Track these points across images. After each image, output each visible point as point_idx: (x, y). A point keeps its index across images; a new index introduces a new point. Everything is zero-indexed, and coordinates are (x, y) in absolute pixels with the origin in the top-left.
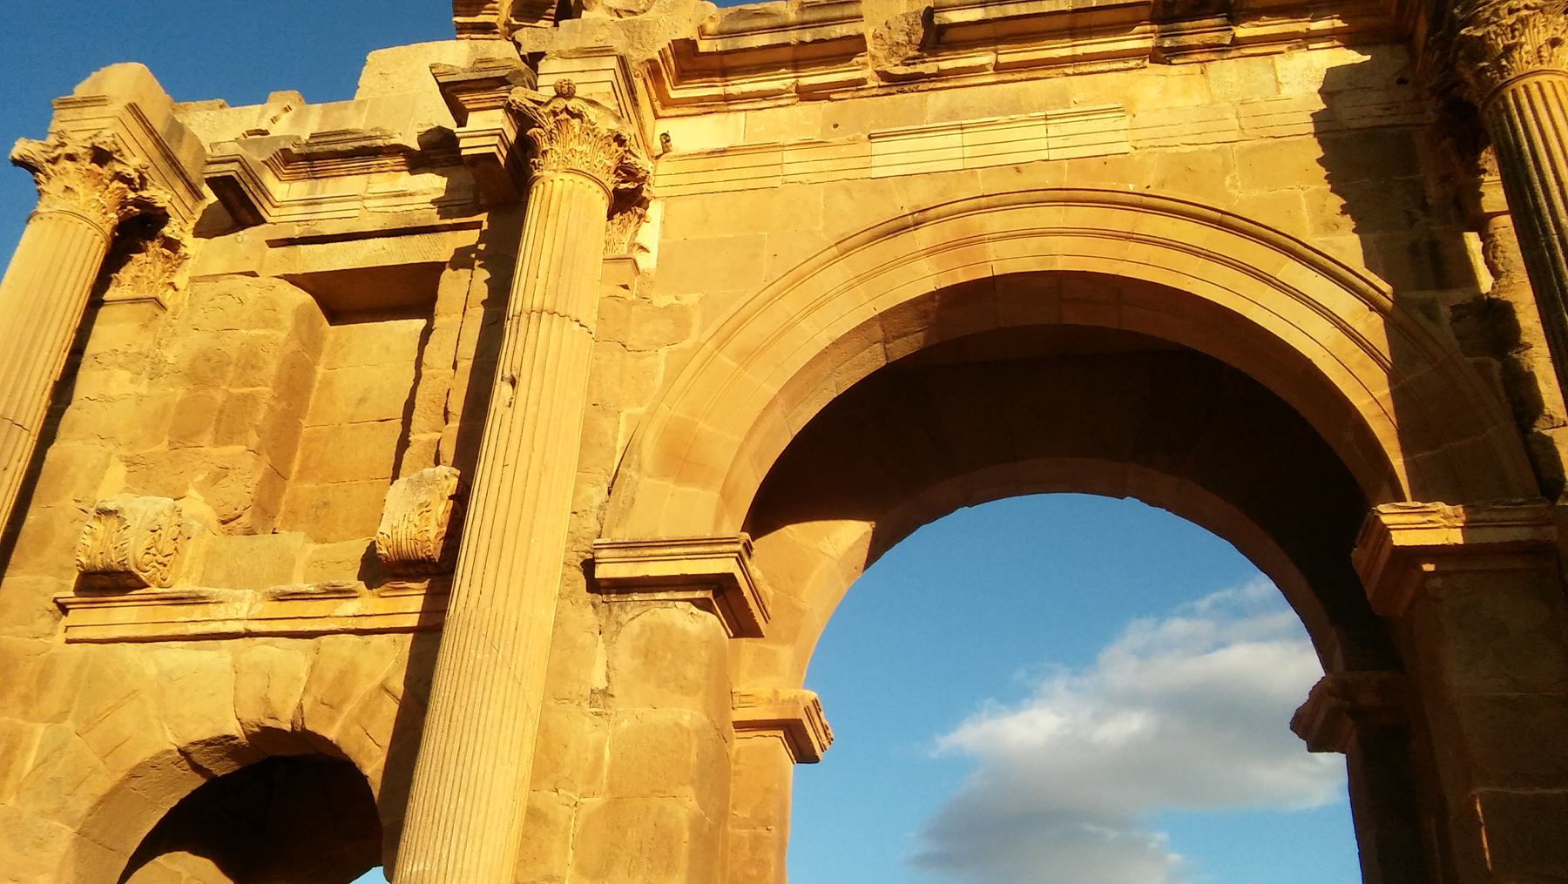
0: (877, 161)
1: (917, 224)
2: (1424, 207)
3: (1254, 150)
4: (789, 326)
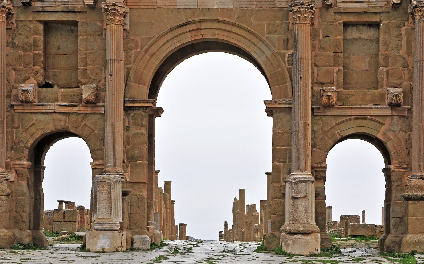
0: (178, 4)
1: (187, 24)
2: (288, 29)
3: (258, 10)
4: (160, 47)
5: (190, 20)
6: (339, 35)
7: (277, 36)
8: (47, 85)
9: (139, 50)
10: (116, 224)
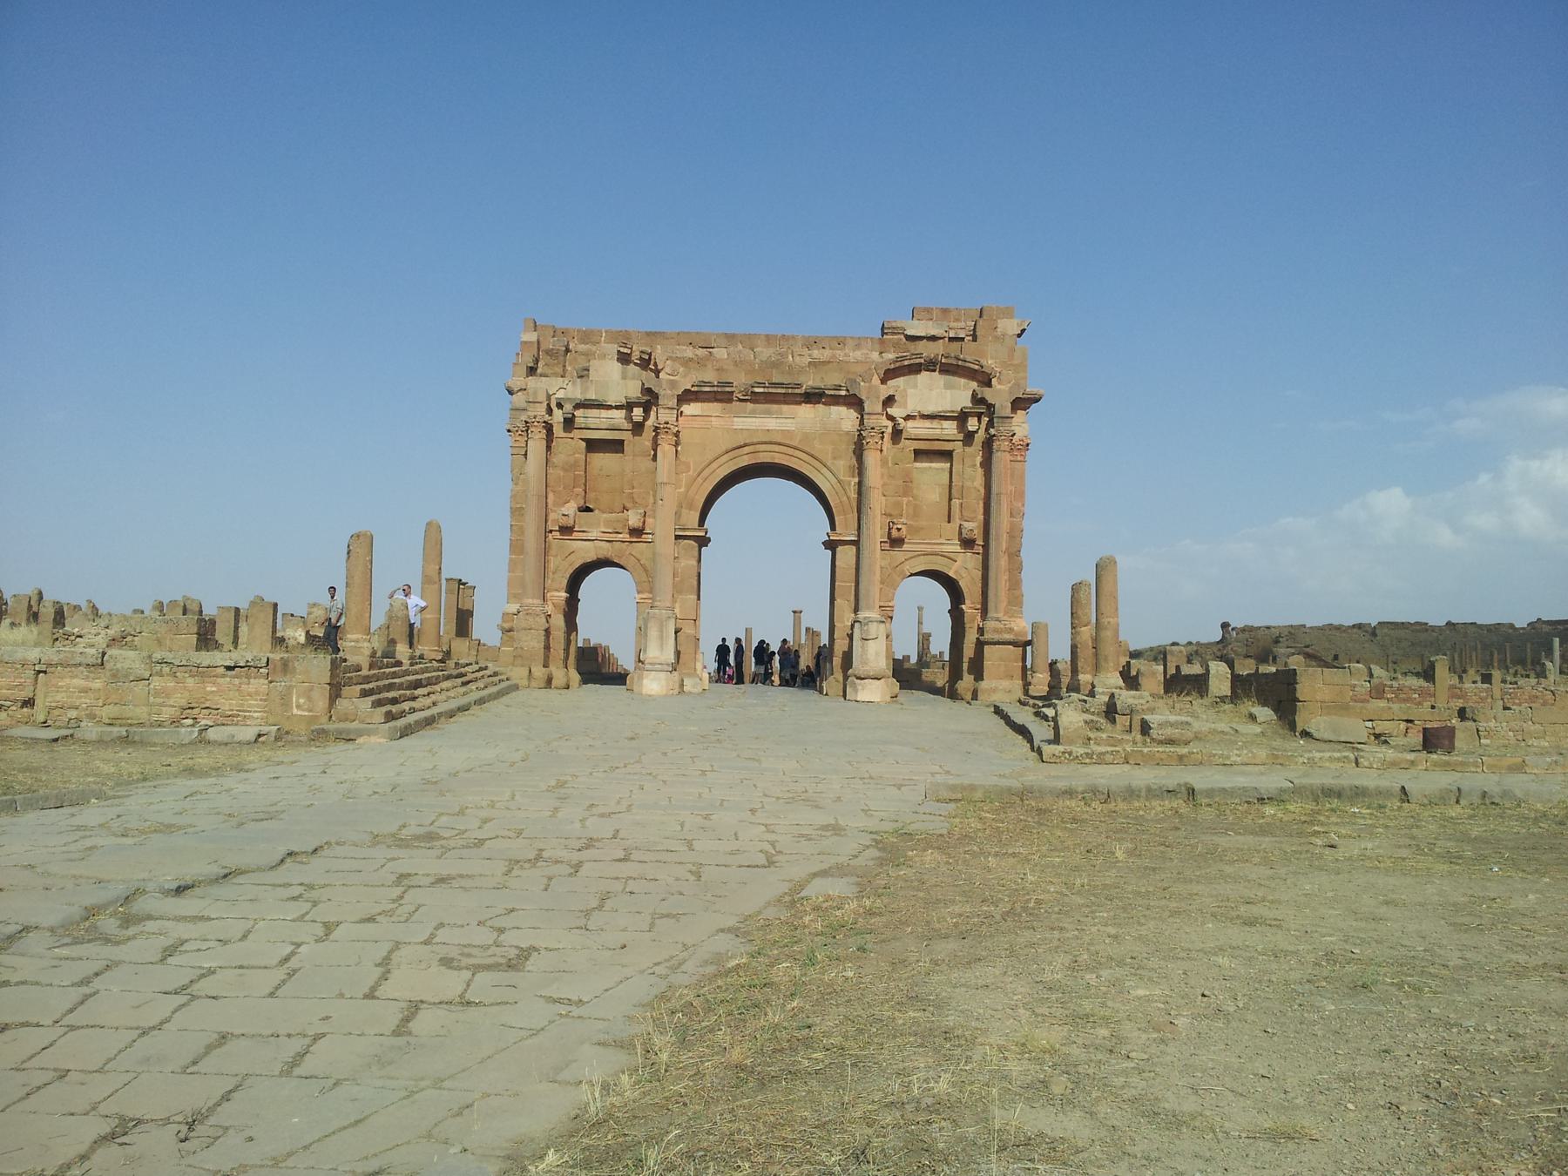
3: (823, 433)
4: (715, 470)
5: (747, 442)
6: (909, 463)
7: (842, 463)
8: (588, 510)
9: (691, 473)
10: (668, 665)
